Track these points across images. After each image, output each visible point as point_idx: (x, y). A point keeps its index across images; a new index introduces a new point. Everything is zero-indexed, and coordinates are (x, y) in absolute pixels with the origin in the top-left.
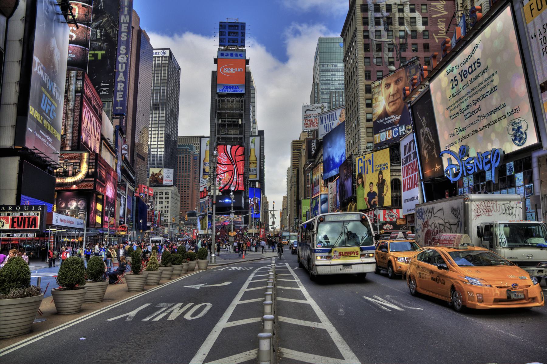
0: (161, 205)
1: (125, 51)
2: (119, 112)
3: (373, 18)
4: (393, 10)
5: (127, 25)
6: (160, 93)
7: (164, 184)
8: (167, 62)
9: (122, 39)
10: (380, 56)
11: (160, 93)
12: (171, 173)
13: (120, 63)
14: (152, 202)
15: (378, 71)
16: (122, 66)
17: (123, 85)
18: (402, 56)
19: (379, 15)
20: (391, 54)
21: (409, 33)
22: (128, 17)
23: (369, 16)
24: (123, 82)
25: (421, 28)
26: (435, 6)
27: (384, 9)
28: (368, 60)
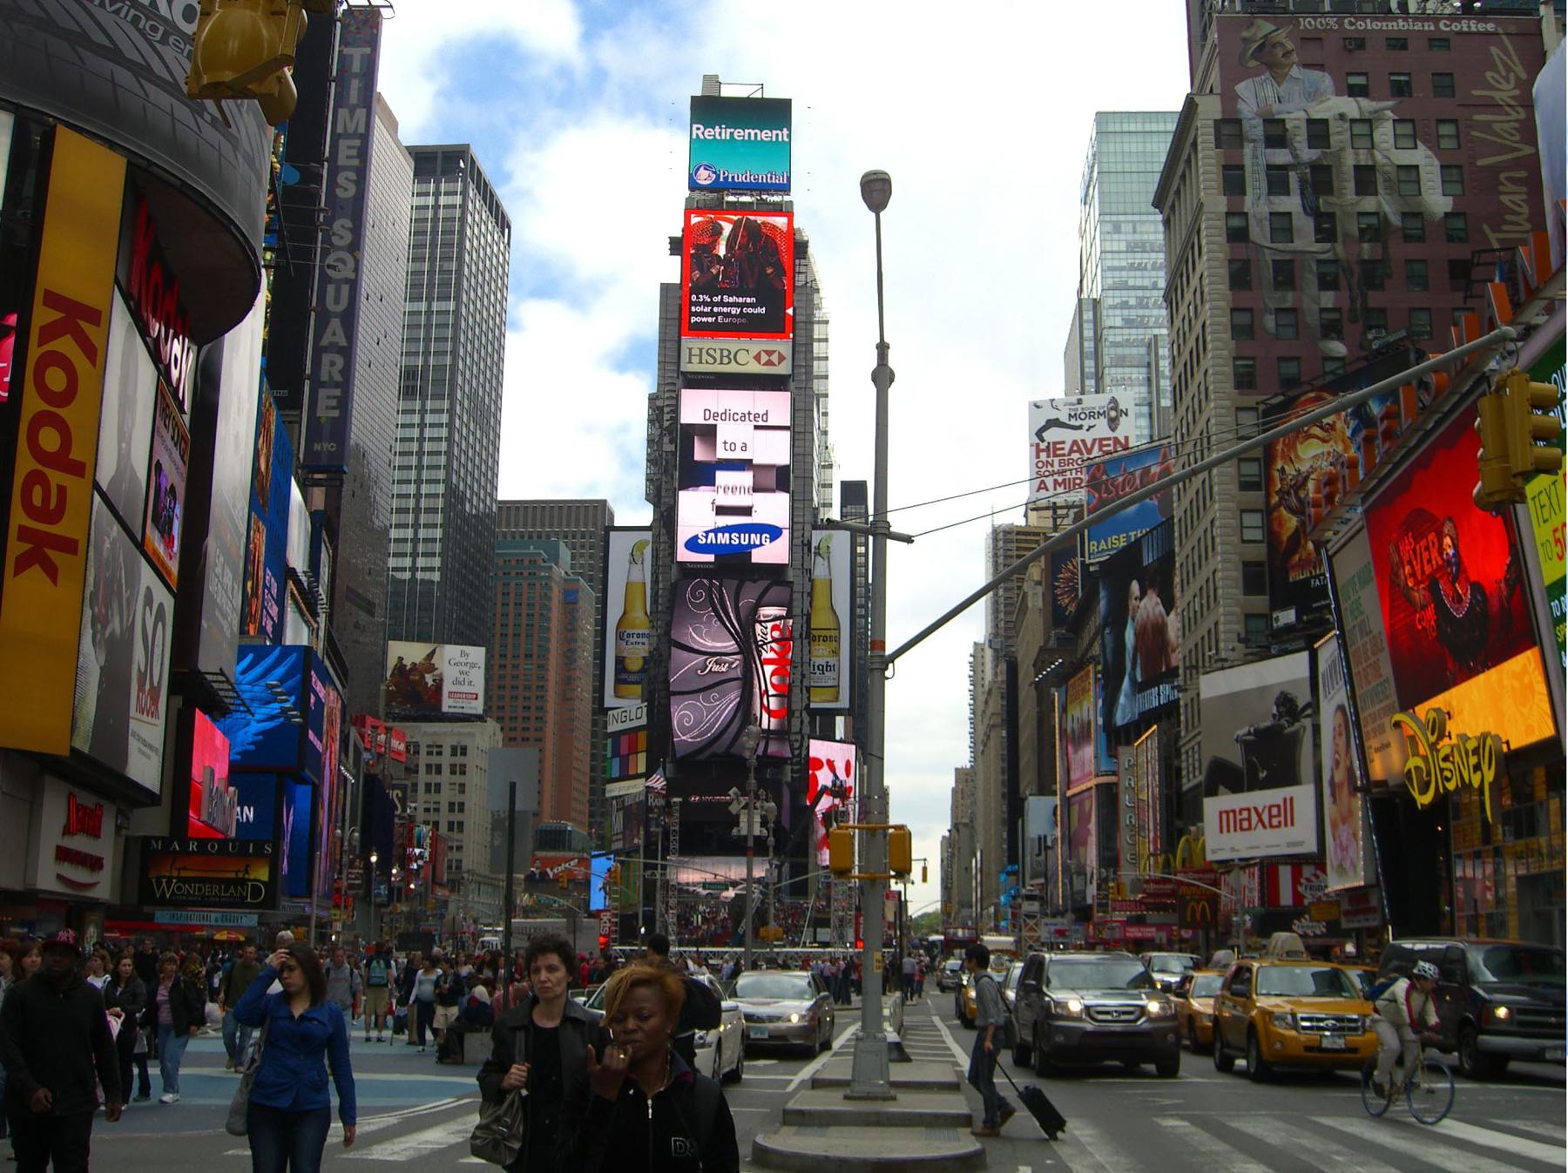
0: (434, 797)
1: (348, 237)
2: (324, 461)
3: (1262, 169)
4: (1333, 139)
5: (357, 143)
7: (445, 709)
9: (339, 192)
10: (1288, 305)
11: (428, 326)
12: (473, 666)
14: (404, 788)
15: (1280, 359)
16: (338, 291)
17: (340, 362)
18: (1371, 304)
19: (1281, 157)
20: (1328, 299)
21: (1395, 220)
23: (1248, 162)
25: (1437, 200)
26: (1487, 127)
27: (1301, 139)
28: (1243, 318)
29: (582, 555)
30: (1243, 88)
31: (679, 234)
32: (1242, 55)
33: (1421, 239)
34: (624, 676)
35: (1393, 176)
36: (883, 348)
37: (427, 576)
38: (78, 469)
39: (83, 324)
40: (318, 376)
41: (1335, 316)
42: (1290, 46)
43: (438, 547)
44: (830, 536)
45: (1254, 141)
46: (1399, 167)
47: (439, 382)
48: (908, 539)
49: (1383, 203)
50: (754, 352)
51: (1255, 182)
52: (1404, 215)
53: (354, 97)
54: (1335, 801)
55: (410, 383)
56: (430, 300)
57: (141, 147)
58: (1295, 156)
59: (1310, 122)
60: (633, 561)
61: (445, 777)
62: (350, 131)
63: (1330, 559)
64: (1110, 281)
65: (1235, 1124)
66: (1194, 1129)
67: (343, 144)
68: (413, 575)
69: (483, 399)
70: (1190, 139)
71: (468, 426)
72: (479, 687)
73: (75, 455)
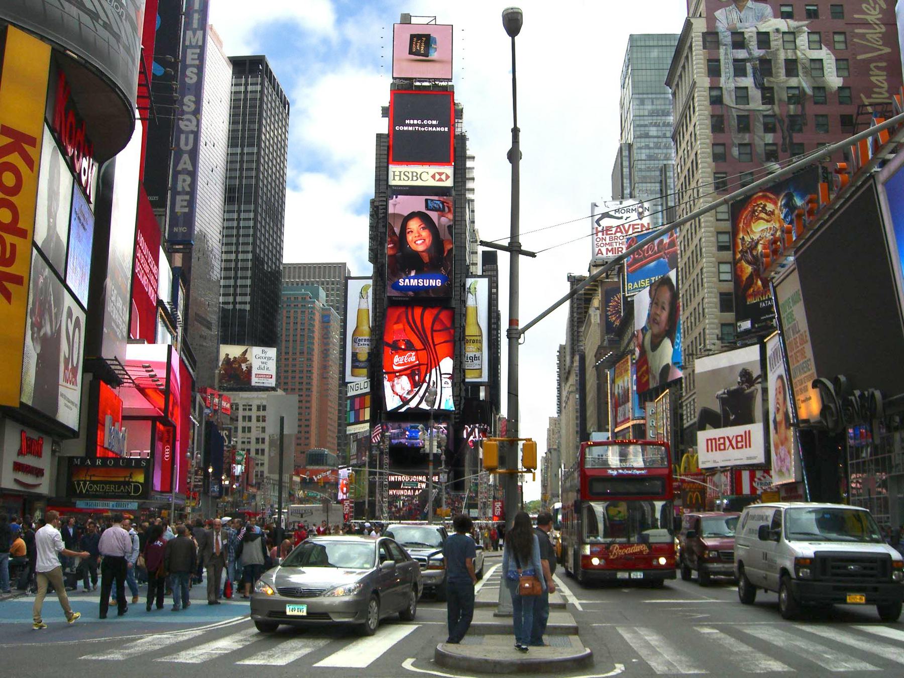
0: (247, 435)
1: (193, 106)
2: (180, 238)
3: (731, 62)
4: (773, 44)
5: (198, 51)
7: (253, 384)
9: (187, 80)
10: (746, 141)
11: (242, 162)
12: (269, 358)
13: (181, 131)
14: (230, 430)
16: (187, 139)
17: (189, 179)
18: (795, 141)
19: (742, 54)
20: (769, 138)
21: (809, 91)
23: (722, 58)
25: (834, 80)
26: (863, 36)
27: (753, 44)
28: (720, 150)
29: (332, 295)
30: (719, 14)
31: (387, 105)
33: (824, 103)
34: (357, 364)
35: (808, 65)
36: (515, 132)
37: (243, 307)
38: (23, 234)
39: (26, 146)
40: (176, 188)
41: (774, 148)
43: (248, 290)
44: (476, 282)
45: (725, 45)
46: (812, 60)
47: (248, 194)
48: (533, 255)
49: (802, 81)
50: (431, 174)
51: (727, 69)
52: (814, 88)
53: (195, 24)
54: (777, 432)
55: (232, 195)
56: (242, 146)
58: (750, 54)
59: (759, 33)
60: (362, 296)
61: (254, 424)
62: (194, 44)
63: (774, 288)
64: (638, 133)
65: (748, 631)
66: (722, 635)
67: (189, 51)
68: (234, 306)
69: (274, 204)
71: (265, 220)
72: (273, 371)
73: (21, 225)
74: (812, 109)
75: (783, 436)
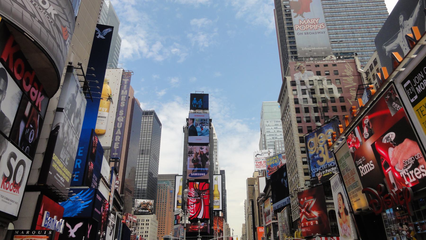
0: (142, 230)
1: (122, 114)
6: (146, 142)
8: (150, 138)
9: (121, 106)
10: (308, 116)
11: (146, 142)
13: (118, 122)
16: (120, 124)
17: (119, 137)
18: (326, 115)
20: (316, 114)
22: (126, 91)
23: (297, 89)
24: (120, 135)
25: (337, 95)
26: (346, 80)
27: (308, 84)
32: (295, 69)
33: (335, 102)
42: (304, 67)
43: (146, 182)
46: (329, 89)
49: (326, 95)
51: (300, 92)
52: (331, 98)
54: (341, 218)
57: (5, 15)
63: (335, 154)
67: (122, 96)
70: (285, 86)
74: (330, 105)
75: (344, 220)
